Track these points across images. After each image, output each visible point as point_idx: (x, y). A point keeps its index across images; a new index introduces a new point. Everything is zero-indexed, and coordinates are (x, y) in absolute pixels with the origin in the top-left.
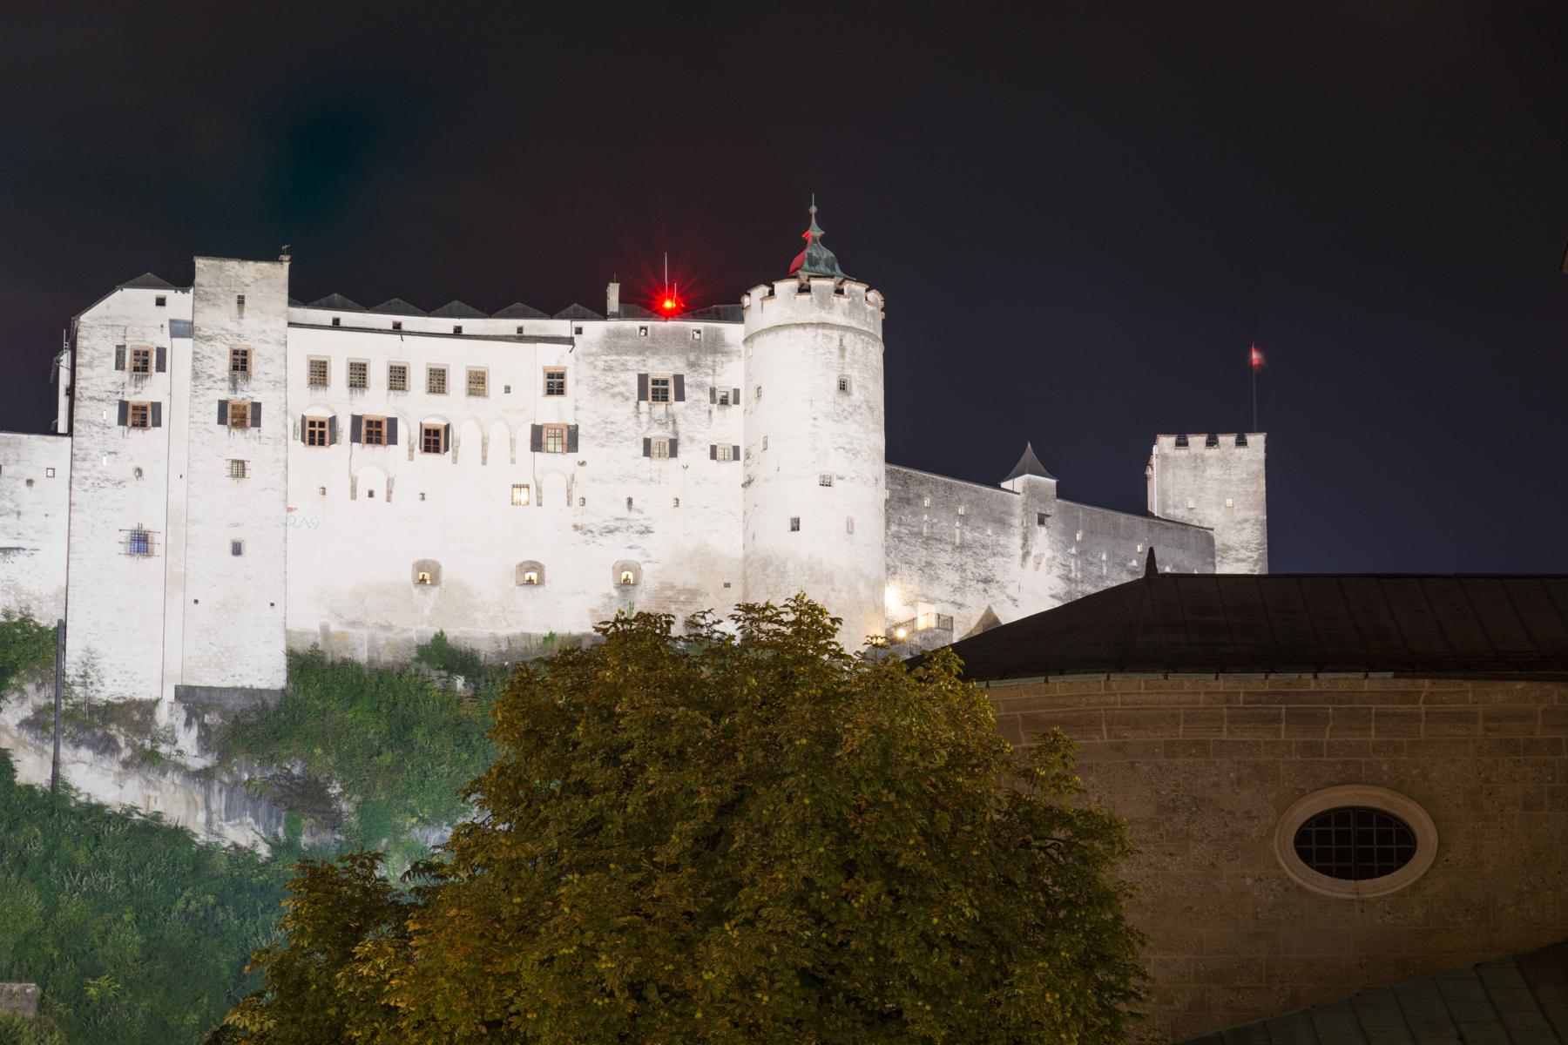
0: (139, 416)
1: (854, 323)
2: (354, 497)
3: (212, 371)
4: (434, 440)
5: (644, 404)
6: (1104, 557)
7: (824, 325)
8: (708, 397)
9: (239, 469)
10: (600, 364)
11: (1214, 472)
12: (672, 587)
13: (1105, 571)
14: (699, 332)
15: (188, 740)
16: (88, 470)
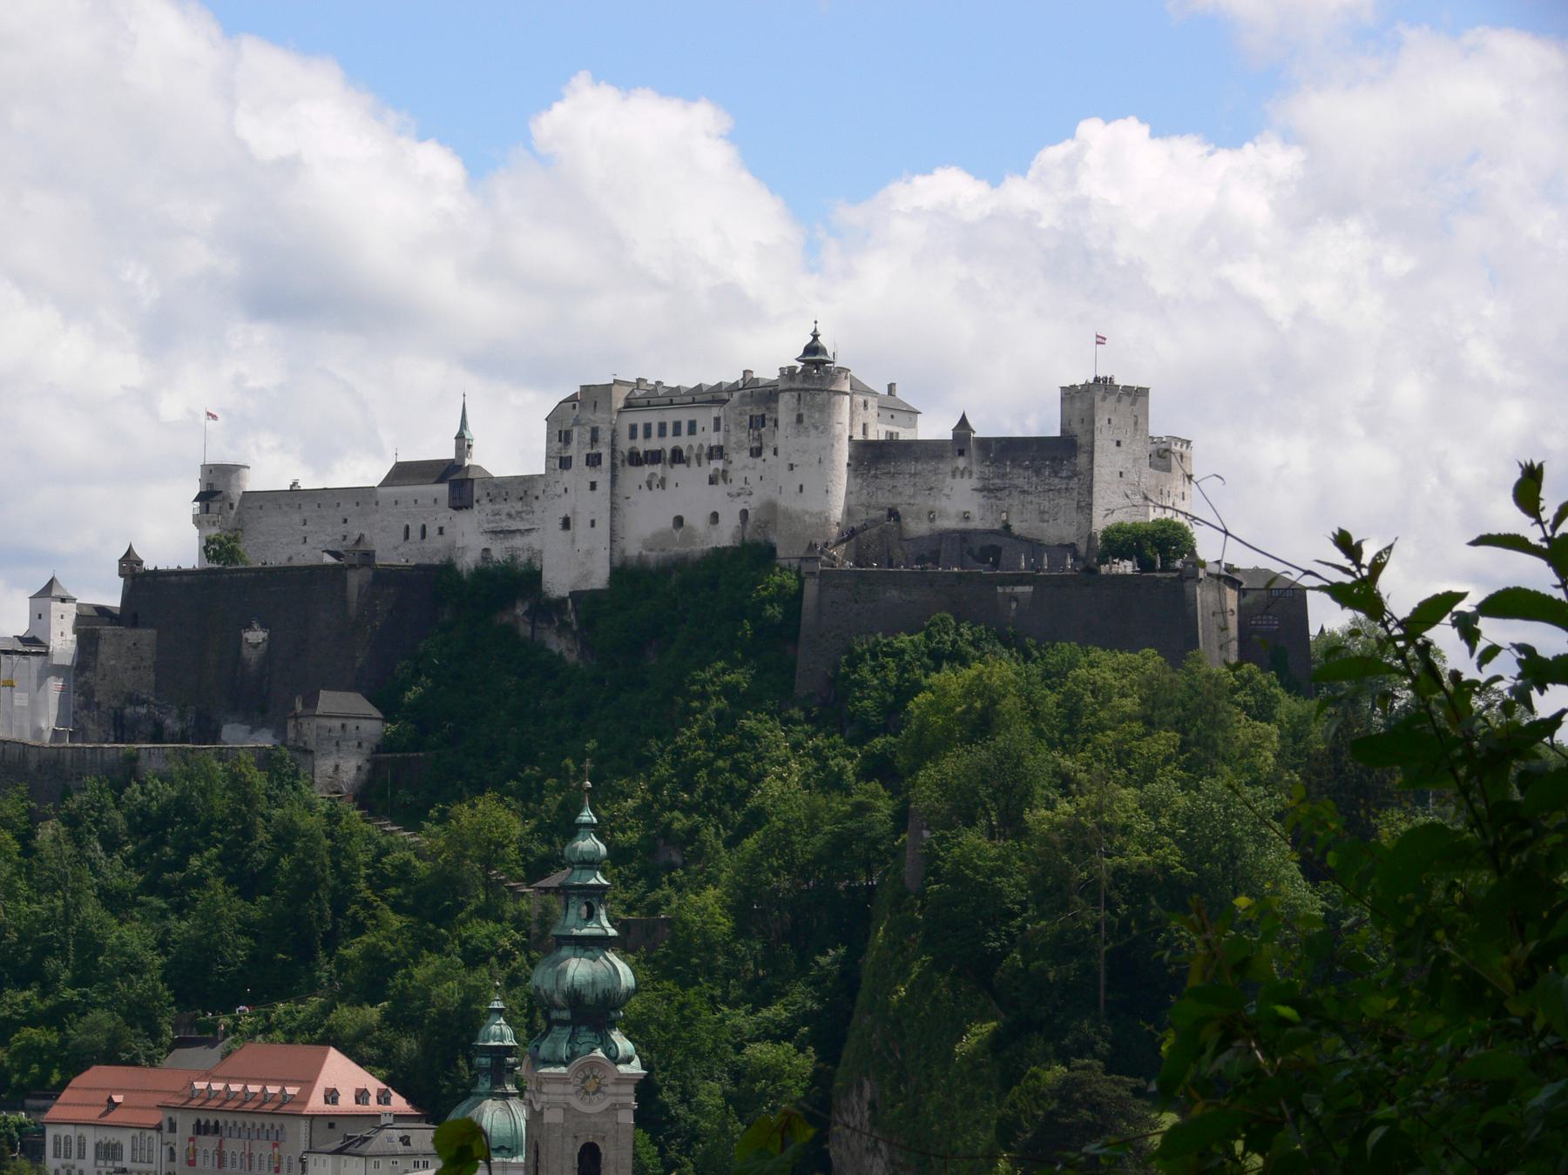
0: (565, 463)
1: (806, 386)
2: (651, 489)
4: (677, 457)
6: (1008, 463)
7: (791, 390)
9: (593, 486)
15: (573, 617)
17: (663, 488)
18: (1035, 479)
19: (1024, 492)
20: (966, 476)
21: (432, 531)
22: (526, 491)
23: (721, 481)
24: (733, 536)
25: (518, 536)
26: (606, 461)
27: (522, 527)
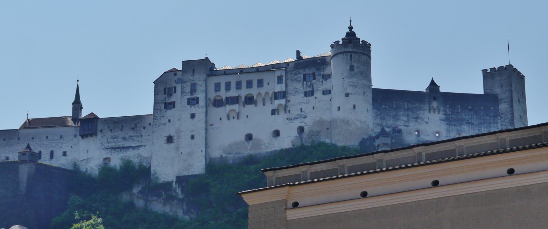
0: (170, 105)
1: (355, 50)
2: (229, 119)
3: (186, 91)
4: (250, 100)
5: (305, 83)
6: (459, 107)
8: (321, 78)
9: (193, 116)
10: (293, 73)
11: (498, 78)
12: (313, 131)
13: (460, 111)
14: (319, 60)
15: (178, 191)
16: (157, 122)
17: (238, 119)
18: (475, 116)
19: (469, 123)
20: (437, 112)
21: (58, 153)
22: (136, 125)
23: (282, 112)
24: (292, 142)
25: (131, 150)
26: (202, 102)
27: (133, 144)
